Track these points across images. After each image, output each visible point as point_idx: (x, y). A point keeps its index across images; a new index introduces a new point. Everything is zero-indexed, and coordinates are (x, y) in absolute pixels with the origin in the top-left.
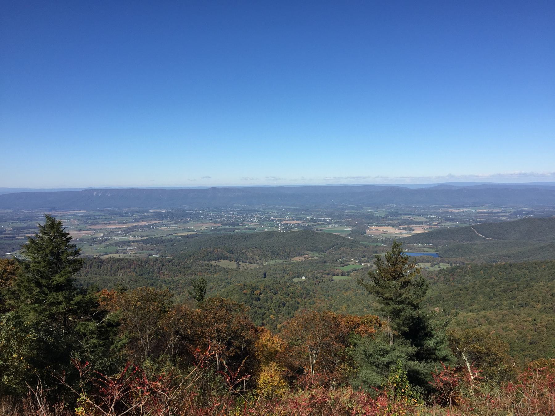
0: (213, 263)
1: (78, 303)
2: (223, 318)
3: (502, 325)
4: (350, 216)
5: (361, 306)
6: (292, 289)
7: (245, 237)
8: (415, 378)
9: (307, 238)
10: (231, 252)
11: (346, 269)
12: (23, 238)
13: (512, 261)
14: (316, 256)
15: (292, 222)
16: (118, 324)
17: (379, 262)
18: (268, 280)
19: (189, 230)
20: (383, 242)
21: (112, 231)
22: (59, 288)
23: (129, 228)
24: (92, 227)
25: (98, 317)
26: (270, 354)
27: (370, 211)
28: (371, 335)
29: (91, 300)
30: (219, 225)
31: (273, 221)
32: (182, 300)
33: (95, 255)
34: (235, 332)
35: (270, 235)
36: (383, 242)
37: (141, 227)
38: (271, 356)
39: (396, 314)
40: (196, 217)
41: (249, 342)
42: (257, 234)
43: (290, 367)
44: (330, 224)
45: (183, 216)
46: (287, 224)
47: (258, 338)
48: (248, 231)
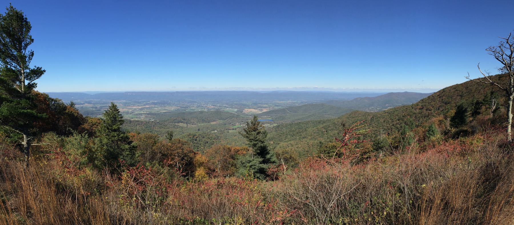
0: (176, 124)
1: (122, 137)
2: (180, 148)
3: (297, 146)
5: (241, 143)
6: (211, 136)
7: (191, 113)
8: (262, 171)
9: (218, 114)
10: (184, 119)
11: (234, 127)
13: (300, 121)
14: (221, 121)
16: (137, 147)
17: (248, 124)
18: (200, 132)
20: (250, 115)
21: (135, 109)
22: (115, 130)
25: (129, 143)
26: (201, 163)
27: (245, 102)
28: (244, 155)
29: (127, 137)
32: (163, 139)
33: (129, 119)
34: (185, 154)
35: (201, 112)
36: (250, 115)
37: (146, 108)
38: (201, 164)
39: (255, 145)
40: (169, 104)
41: (191, 158)
42: (196, 112)
43: (209, 169)
45: (163, 104)
47: (195, 157)
48: (192, 111)
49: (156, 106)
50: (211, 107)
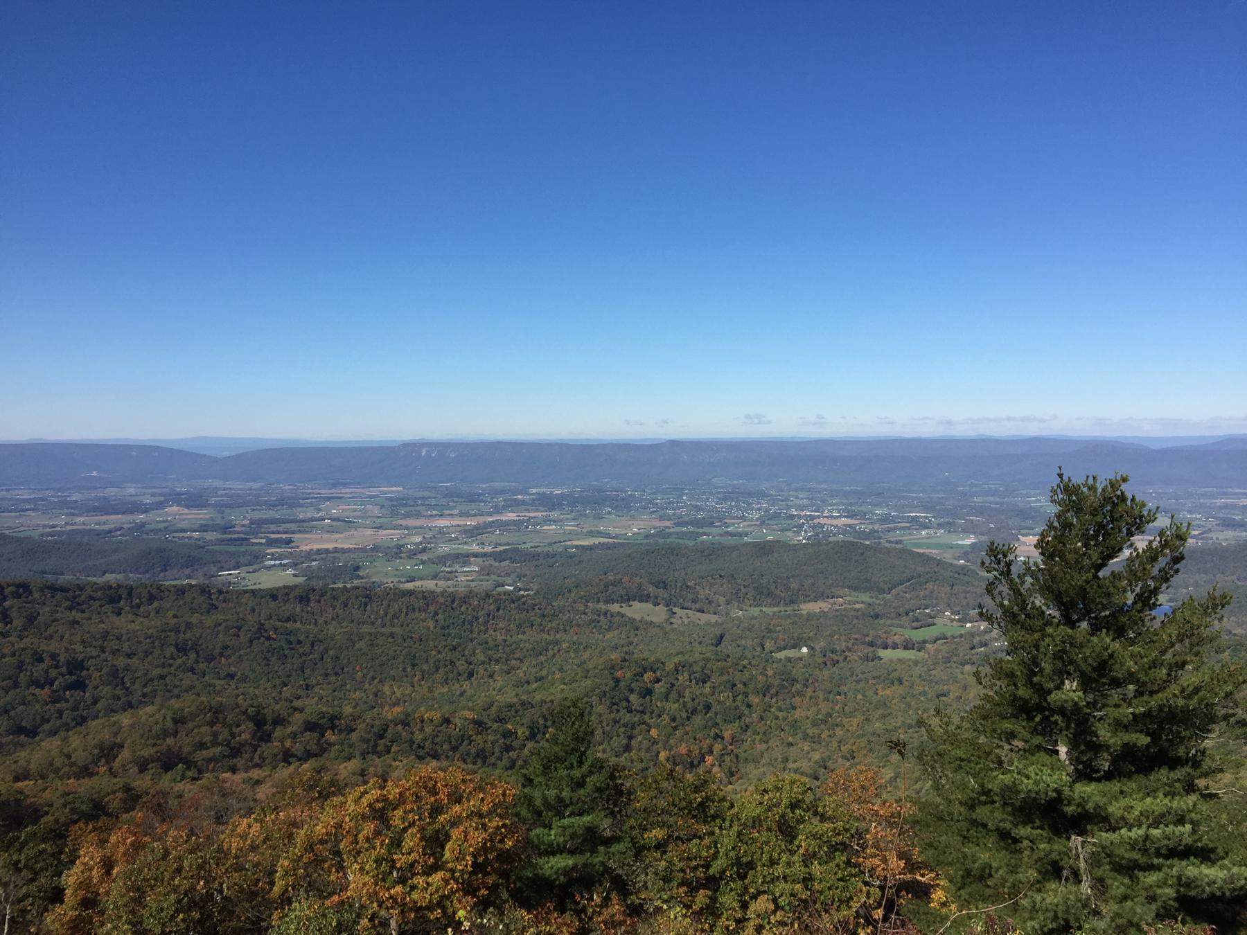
4: (980, 511)
12: (263, 541)
15: (834, 522)
19: (600, 534)
21: (441, 531)
23: (477, 528)
24: (404, 522)
30: (668, 523)
31: (793, 517)
37: (503, 525)
44: (924, 527)
46: (822, 526)
48: (730, 541)
49: (555, 515)
50: (835, 521)
